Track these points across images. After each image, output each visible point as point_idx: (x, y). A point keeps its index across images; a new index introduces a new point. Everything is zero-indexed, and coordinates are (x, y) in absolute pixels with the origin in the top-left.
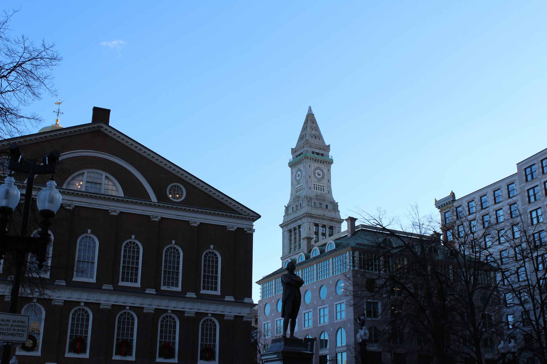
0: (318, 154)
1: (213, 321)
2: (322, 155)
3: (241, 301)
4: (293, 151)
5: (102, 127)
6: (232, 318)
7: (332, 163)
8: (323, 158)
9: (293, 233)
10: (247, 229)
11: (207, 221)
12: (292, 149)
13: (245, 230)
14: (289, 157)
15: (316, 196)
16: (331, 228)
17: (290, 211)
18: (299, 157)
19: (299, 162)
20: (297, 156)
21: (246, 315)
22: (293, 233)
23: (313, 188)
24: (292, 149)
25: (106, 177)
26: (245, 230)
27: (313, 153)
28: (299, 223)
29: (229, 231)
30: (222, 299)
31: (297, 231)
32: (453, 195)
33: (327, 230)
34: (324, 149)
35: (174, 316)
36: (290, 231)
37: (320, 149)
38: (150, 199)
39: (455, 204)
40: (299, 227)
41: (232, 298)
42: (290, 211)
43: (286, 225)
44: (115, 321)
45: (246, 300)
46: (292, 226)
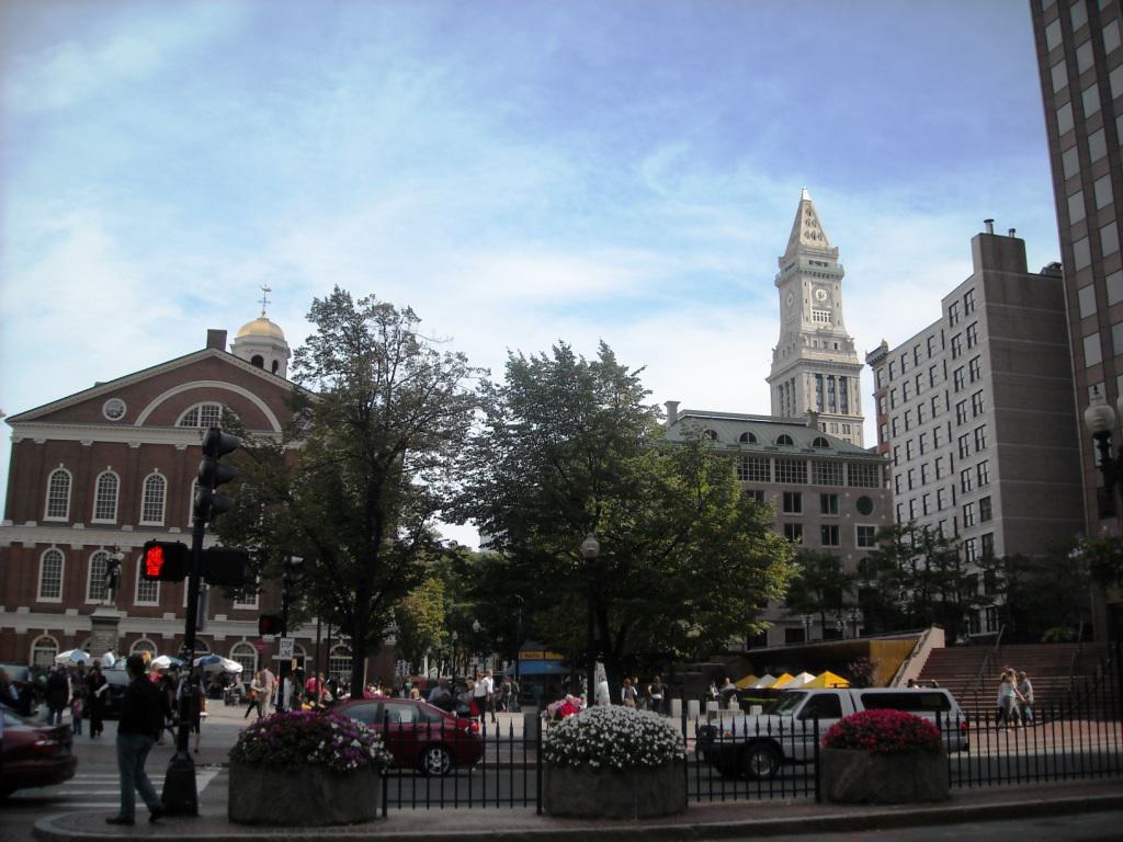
0: (819, 264)
2: (826, 265)
4: (782, 261)
7: (842, 277)
8: (827, 269)
9: (785, 391)
12: (780, 258)
14: (775, 270)
15: (817, 331)
16: (843, 379)
17: (781, 356)
18: (790, 270)
19: (790, 278)
20: (786, 270)
22: (785, 391)
23: (812, 318)
24: (780, 258)
27: (811, 262)
28: (792, 374)
31: (790, 388)
32: (884, 345)
33: (838, 382)
34: (827, 256)
36: (781, 388)
37: (822, 256)
38: (272, 429)
39: (889, 359)
40: (793, 380)
42: (781, 356)
43: (775, 379)
46: (782, 381)
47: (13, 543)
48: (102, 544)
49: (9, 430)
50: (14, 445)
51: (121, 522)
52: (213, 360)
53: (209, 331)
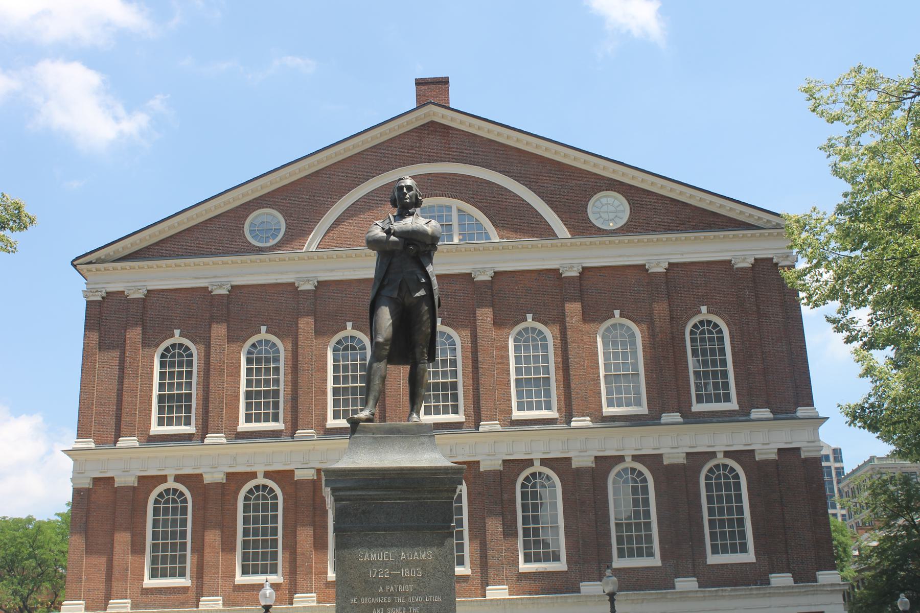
1: (731, 468)
3: (789, 415)
5: (434, 114)
6: (774, 456)
10: (778, 257)
11: (685, 256)
13: (775, 261)
21: (805, 444)
25: (459, 210)
26: (775, 261)
29: (737, 269)
30: (744, 418)
35: (640, 467)
41: (766, 411)
44: (514, 493)
45: (802, 412)
47: (96, 480)
48: (260, 469)
49: (80, 283)
50: (89, 304)
51: (294, 425)
52: (432, 127)
53: (419, 83)
